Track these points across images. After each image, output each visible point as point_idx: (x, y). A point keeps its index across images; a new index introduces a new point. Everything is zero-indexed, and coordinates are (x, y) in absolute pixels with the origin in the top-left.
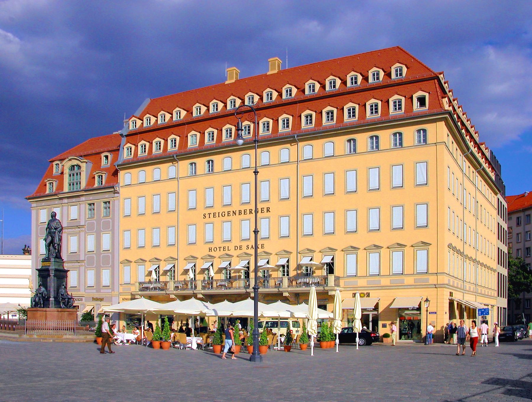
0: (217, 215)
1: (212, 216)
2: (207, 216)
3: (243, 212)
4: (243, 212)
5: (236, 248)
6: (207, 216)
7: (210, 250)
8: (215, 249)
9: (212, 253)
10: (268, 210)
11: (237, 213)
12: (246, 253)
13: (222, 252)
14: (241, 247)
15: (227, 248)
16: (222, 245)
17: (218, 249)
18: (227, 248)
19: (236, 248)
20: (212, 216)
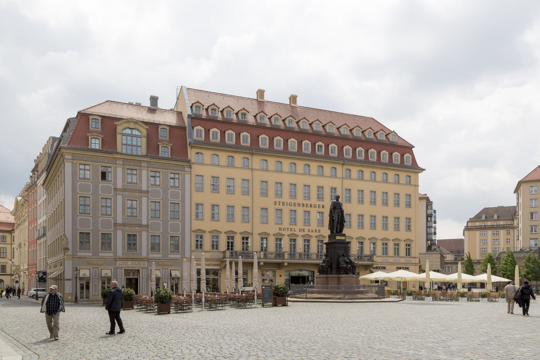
0: (285, 204)
1: (281, 204)
2: (278, 203)
3: (305, 205)
4: (305, 205)
5: (300, 230)
6: (278, 203)
7: (280, 229)
9: (282, 232)
10: (323, 207)
11: (301, 205)
12: (308, 235)
13: (290, 232)
14: (304, 230)
16: (290, 227)
17: (287, 230)
20: (281, 204)
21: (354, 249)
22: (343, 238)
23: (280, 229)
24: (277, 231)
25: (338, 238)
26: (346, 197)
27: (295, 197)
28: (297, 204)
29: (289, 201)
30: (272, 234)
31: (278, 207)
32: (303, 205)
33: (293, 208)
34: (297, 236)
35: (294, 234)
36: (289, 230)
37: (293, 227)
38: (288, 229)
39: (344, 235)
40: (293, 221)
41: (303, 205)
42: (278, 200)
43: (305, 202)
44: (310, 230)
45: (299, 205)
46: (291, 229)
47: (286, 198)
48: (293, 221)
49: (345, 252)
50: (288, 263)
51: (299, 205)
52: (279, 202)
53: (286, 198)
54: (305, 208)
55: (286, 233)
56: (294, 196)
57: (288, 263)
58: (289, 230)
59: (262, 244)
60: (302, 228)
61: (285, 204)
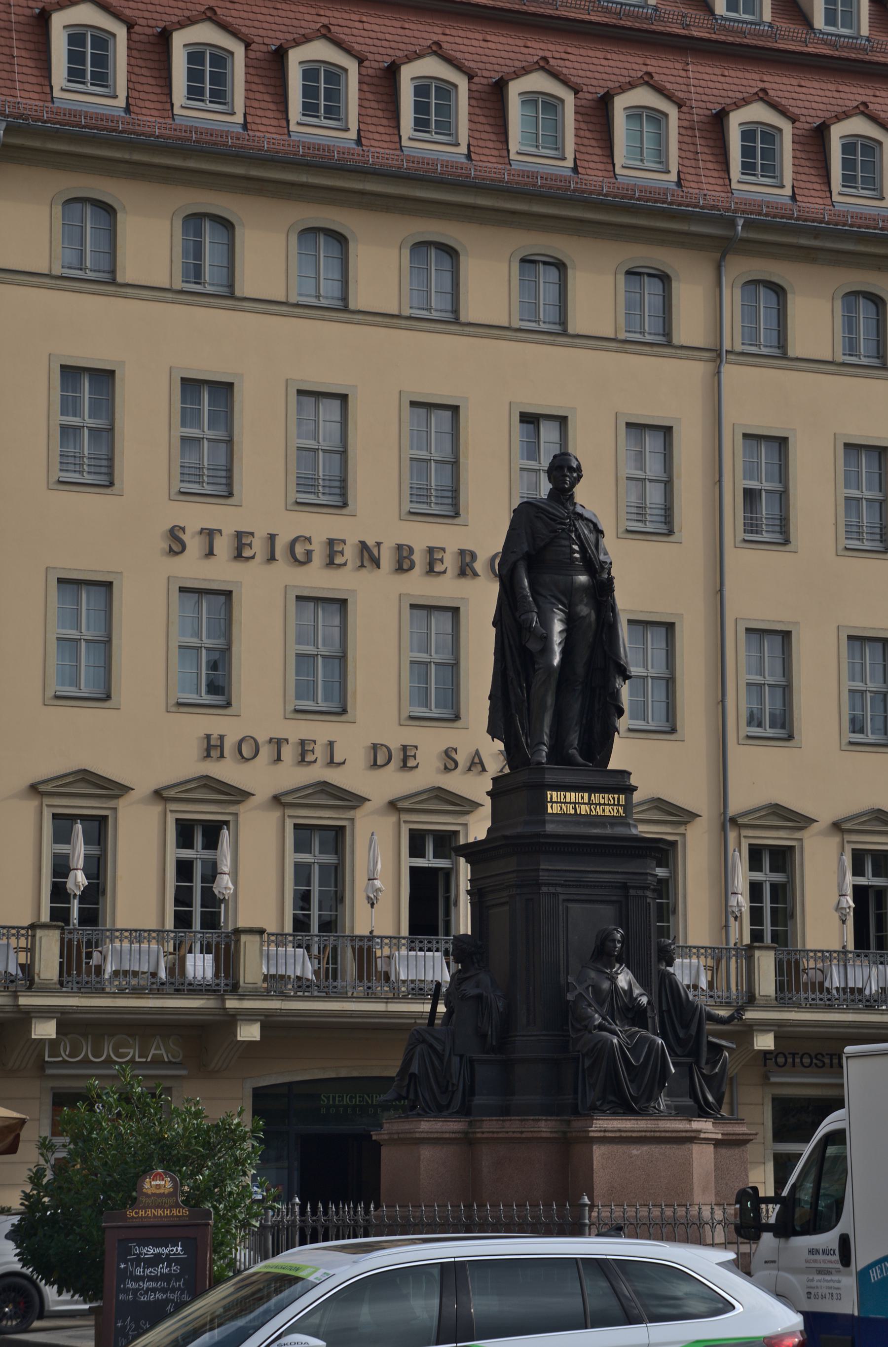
0: (258, 547)
1: (223, 546)
2: (194, 545)
3: (419, 558)
4: (419, 558)
5: (377, 757)
7: (212, 748)
8: (246, 751)
11: (387, 558)
13: (292, 776)
14: (407, 758)
15: (320, 752)
16: (298, 730)
17: (265, 752)
18: (320, 752)
19: (377, 757)
20: (223, 546)
21: (706, 902)
22: (605, 805)
23: (212, 748)
24: (189, 765)
25: (559, 803)
26: (751, 496)
27: (340, 498)
28: (350, 553)
29: (290, 525)
30: (143, 778)
31: (193, 568)
32: (403, 561)
33: (316, 579)
34: (351, 800)
35: (325, 788)
36: (289, 753)
37: (320, 731)
38: (278, 743)
39: (620, 784)
40: (324, 681)
41: (403, 561)
42: (195, 516)
43: (421, 536)
44: (462, 758)
45: (368, 556)
46: (304, 749)
47: (264, 495)
48: (324, 681)
49: (623, 921)
50: (271, 1024)
51: (368, 556)
52: (210, 534)
53: (264, 495)
54: (418, 586)
55: (261, 778)
56: (327, 482)
57: (271, 1024)
58: (289, 753)
59: (61, 868)
60: (395, 737)
61: (258, 547)
